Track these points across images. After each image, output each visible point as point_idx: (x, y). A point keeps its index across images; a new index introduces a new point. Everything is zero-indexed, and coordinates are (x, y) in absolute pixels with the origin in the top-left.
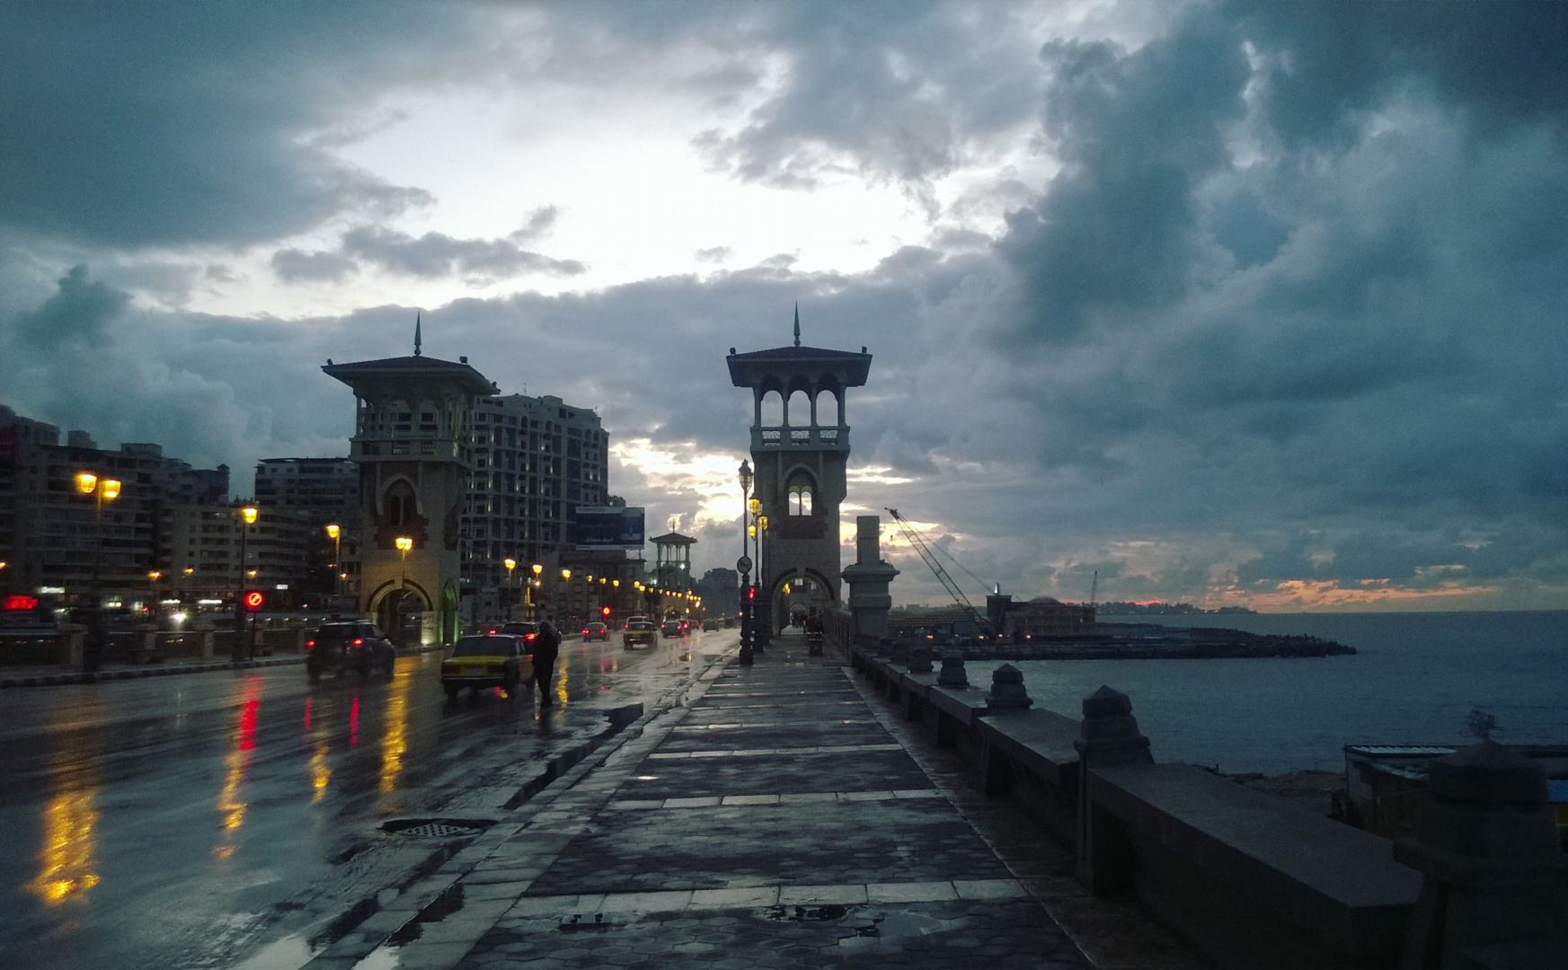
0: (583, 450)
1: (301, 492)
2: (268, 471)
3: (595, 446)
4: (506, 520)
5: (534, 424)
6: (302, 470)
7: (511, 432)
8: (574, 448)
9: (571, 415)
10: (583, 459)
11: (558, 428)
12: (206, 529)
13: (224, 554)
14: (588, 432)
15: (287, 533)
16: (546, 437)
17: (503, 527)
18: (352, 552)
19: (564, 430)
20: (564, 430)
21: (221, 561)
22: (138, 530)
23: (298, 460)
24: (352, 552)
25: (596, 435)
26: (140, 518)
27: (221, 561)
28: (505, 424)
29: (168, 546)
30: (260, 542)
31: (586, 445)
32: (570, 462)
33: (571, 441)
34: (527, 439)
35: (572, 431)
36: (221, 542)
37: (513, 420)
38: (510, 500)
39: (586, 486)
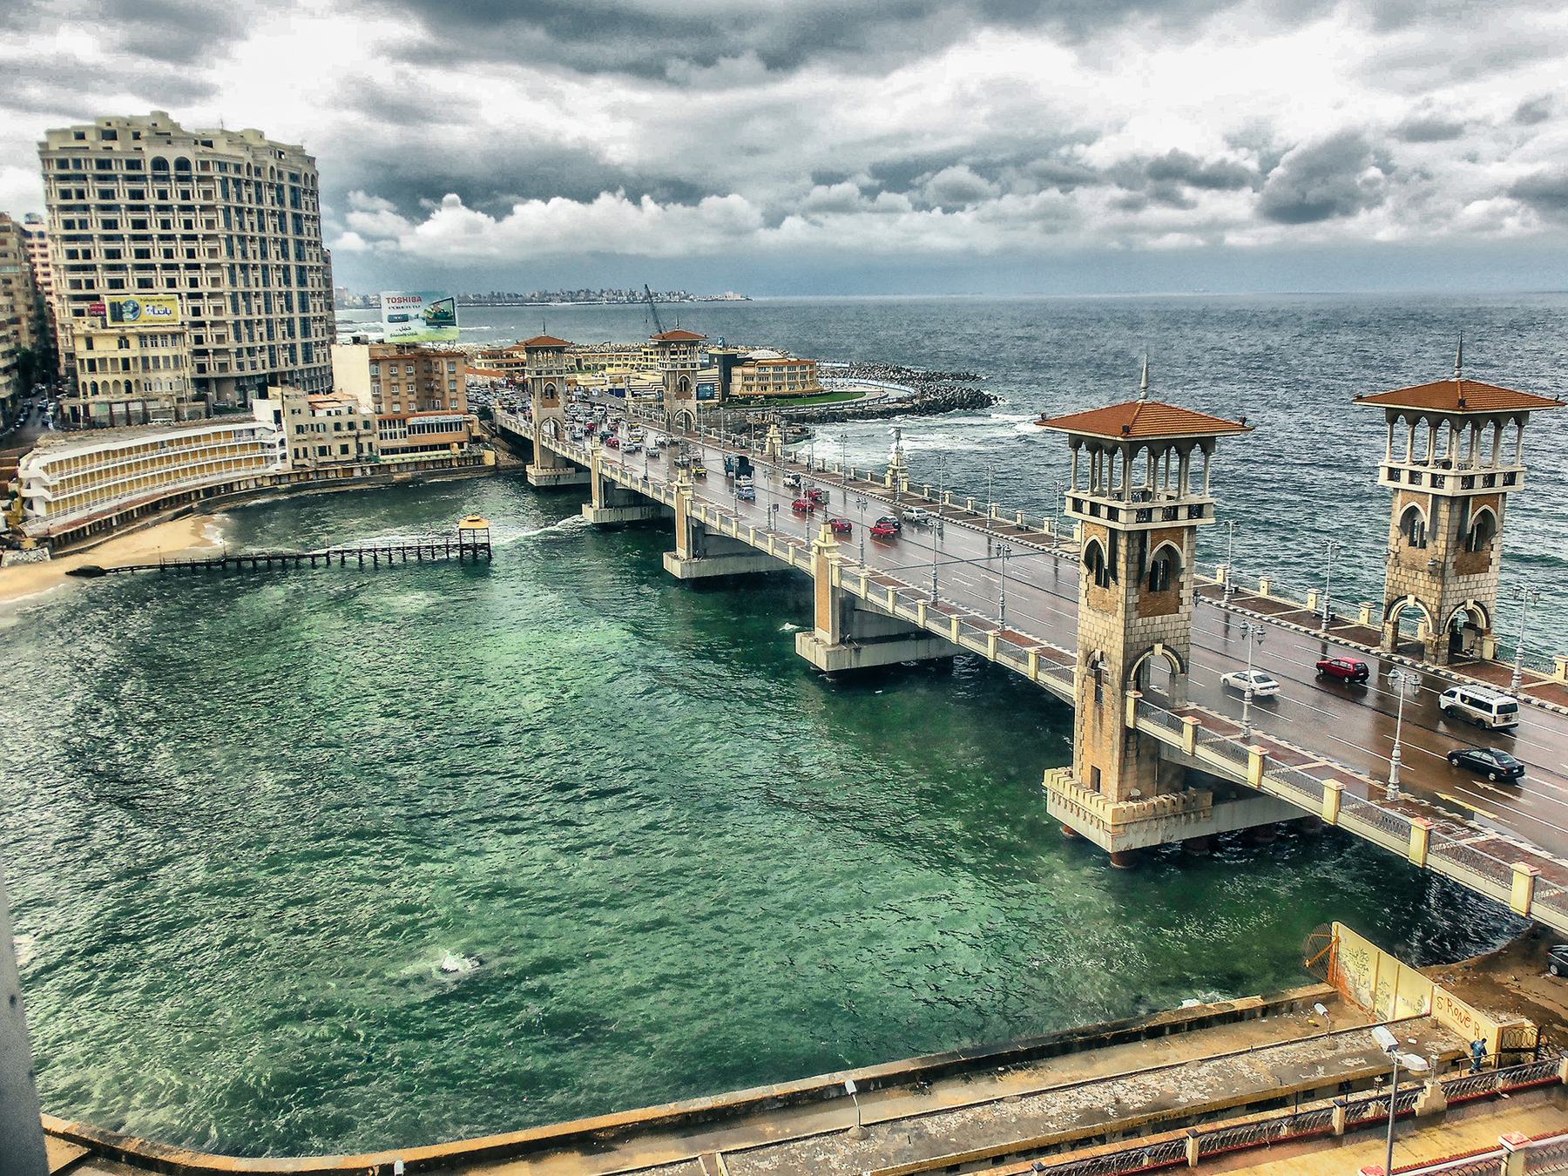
7: (237, 182)
16: (271, 186)
18: (90, 346)
19: (286, 176)
20: (286, 176)
24: (90, 346)
31: (305, 192)
33: (293, 189)
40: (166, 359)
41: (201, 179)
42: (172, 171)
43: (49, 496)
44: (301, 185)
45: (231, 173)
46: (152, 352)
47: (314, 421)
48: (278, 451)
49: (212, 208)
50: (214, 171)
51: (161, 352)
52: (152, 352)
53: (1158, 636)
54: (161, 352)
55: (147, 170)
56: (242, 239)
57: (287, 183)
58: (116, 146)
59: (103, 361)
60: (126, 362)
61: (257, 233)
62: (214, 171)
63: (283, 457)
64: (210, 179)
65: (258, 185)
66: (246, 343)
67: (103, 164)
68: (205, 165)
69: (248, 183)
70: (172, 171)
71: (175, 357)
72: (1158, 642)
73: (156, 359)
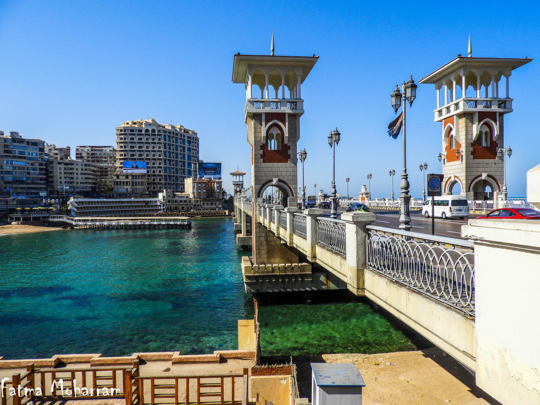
1: (92, 158)
2: (80, 150)
3: (195, 143)
5: (177, 134)
6: (92, 150)
7: (169, 137)
11: (184, 136)
12: (65, 169)
13: (72, 178)
15: (93, 171)
16: (181, 139)
20: (186, 137)
21: (72, 180)
22: (40, 169)
23: (90, 147)
26: (41, 164)
27: (72, 180)
28: (167, 134)
29: (51, 175)
30: (85, 174)
33: (188, 141)
34: (174, 139)
35: (188, 137)
36: (71, 173)
37: (170, 133)
38: (169, 160)
39: (193, 156)
40: (139, 182)
41: (158, 135)
42: (150, 133)
43: (76, 210)
44: (192, 140)
45: (167, 134)
46: (135, 180)
47: (174, 199)
48: (162, 208)
50: (162, 133)
51: (138, 180)
52: (135, 180)
53: (276, 174)
54: (138, 180)
55: (144, 132)
57: (186, 139)
58: (136, 126)
59: (120, 182)
60: (127, 182)
61: (175, 151)
62: (162, 133)
63: (164, 209)
64: (161, 135)
65: (176, 138)
66: (168, 181)
67: (132, 131)
68: (159, 131)
69: (173, 137)
70: (150, 133)
71: (142, 182)
72: (276, 177)
73: (136, 182)
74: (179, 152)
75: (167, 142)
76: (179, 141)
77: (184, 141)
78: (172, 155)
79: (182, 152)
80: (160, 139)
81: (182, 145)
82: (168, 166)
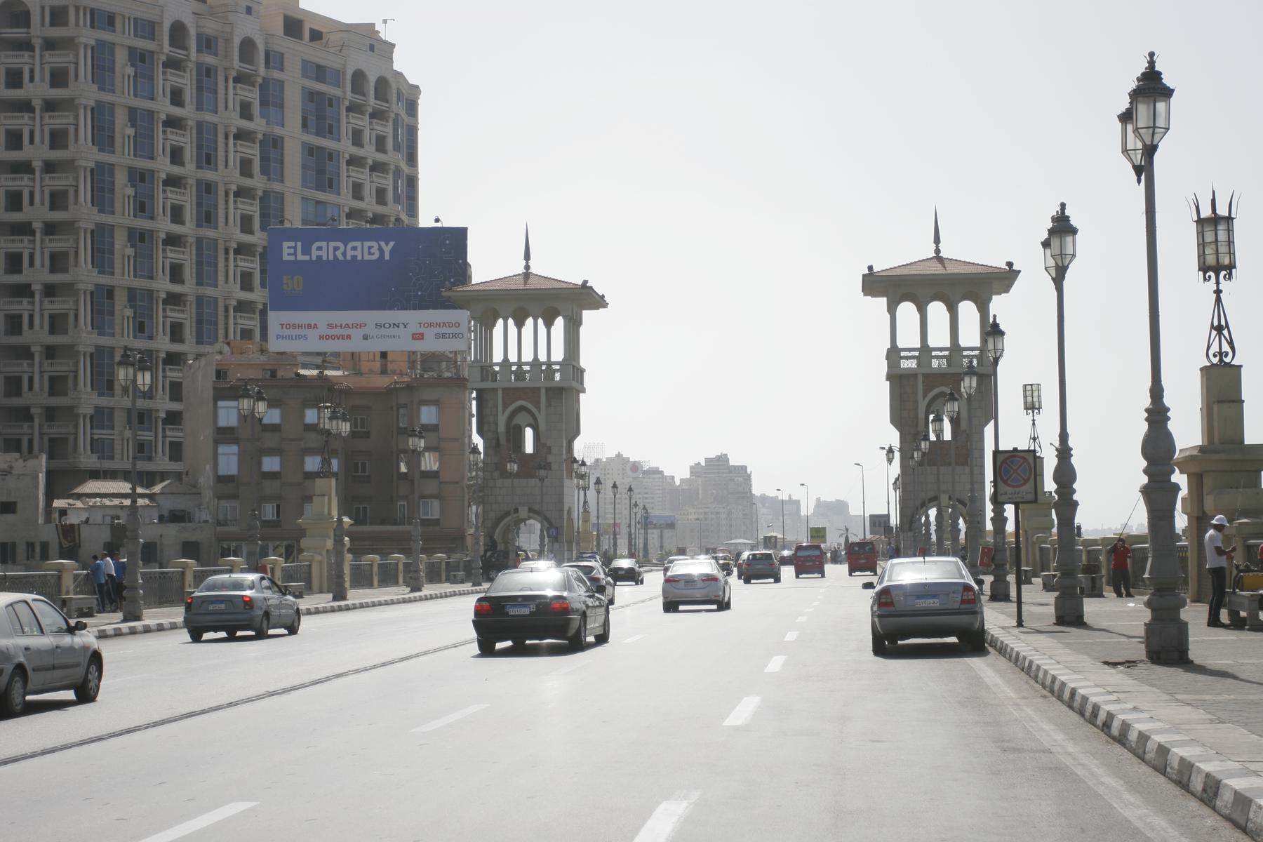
0: (347, 123)
3: (377, 115)
4: (132, 293)
5: (207, 44)
7: (140, 58)
8: (320, 113)
9: (316, 36)
10: (345, 147)
14: (359, 77)
17: (122, 310)
25: (382, 84)
28: (123, 39)
32: (310, 150)
33: (312, 96)
34: (187, 82)
35: (320, 72)
37: (147, 28)
38: (139, 237)
49: (66, 105)
56: (140, 177)
61: (189, 169)
65: (206, 72)
74: (227, 176)
75: (123, 98)
76: (233, 95)
77: (271, 97)
78: (163, 198)
79: (258, 182)
80: (58, 78)
81: (258, 125)
82: (123, 278)
